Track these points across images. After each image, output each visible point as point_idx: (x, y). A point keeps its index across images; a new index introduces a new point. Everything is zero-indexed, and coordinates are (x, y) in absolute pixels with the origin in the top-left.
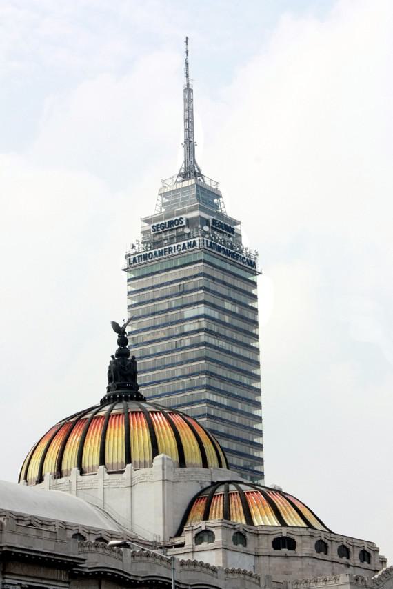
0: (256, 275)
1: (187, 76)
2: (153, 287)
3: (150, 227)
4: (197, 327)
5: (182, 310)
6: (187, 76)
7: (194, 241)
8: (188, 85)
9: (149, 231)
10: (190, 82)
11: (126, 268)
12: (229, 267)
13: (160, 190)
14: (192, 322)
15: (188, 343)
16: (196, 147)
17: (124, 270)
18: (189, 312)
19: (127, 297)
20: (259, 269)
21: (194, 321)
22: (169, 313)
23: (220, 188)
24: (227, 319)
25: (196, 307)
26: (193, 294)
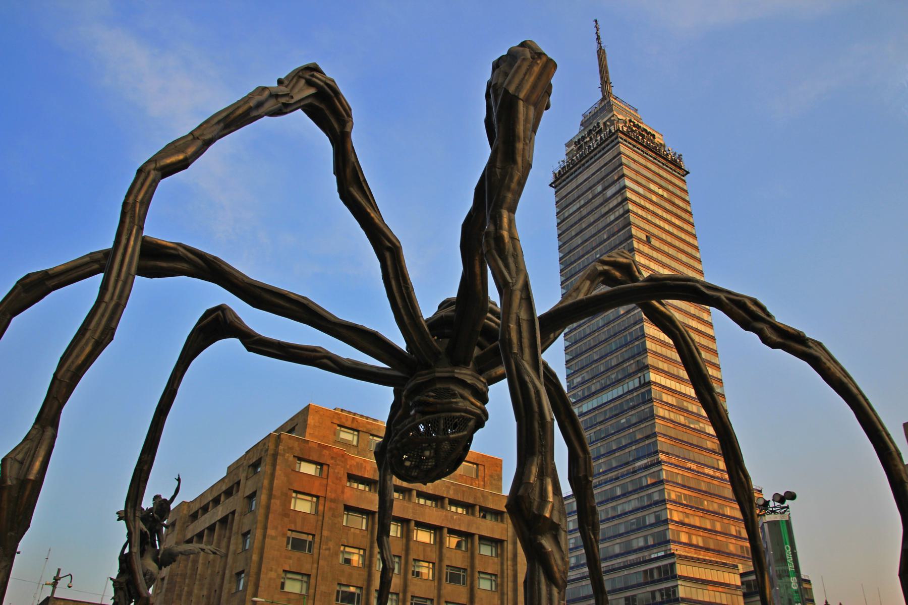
1: (599, 43)
2: (577, 187)
3: (573, 147)
4: (620, 199)
5: (604, 192)
6: (599, 43)
7: (610, 129)
9: (573, 149)
10: (602, 45)
11: (552, 181)
12: (653, 167)
13: (582, 121)
14: (615, 197)
17: (551, 185)
18: (609, 192)
19: (555, 206)
20: (685, 165)
21: (617, 196)
22: (593, 201)
24: (654, 198)
25: (618, 182)
26: (613, 173)
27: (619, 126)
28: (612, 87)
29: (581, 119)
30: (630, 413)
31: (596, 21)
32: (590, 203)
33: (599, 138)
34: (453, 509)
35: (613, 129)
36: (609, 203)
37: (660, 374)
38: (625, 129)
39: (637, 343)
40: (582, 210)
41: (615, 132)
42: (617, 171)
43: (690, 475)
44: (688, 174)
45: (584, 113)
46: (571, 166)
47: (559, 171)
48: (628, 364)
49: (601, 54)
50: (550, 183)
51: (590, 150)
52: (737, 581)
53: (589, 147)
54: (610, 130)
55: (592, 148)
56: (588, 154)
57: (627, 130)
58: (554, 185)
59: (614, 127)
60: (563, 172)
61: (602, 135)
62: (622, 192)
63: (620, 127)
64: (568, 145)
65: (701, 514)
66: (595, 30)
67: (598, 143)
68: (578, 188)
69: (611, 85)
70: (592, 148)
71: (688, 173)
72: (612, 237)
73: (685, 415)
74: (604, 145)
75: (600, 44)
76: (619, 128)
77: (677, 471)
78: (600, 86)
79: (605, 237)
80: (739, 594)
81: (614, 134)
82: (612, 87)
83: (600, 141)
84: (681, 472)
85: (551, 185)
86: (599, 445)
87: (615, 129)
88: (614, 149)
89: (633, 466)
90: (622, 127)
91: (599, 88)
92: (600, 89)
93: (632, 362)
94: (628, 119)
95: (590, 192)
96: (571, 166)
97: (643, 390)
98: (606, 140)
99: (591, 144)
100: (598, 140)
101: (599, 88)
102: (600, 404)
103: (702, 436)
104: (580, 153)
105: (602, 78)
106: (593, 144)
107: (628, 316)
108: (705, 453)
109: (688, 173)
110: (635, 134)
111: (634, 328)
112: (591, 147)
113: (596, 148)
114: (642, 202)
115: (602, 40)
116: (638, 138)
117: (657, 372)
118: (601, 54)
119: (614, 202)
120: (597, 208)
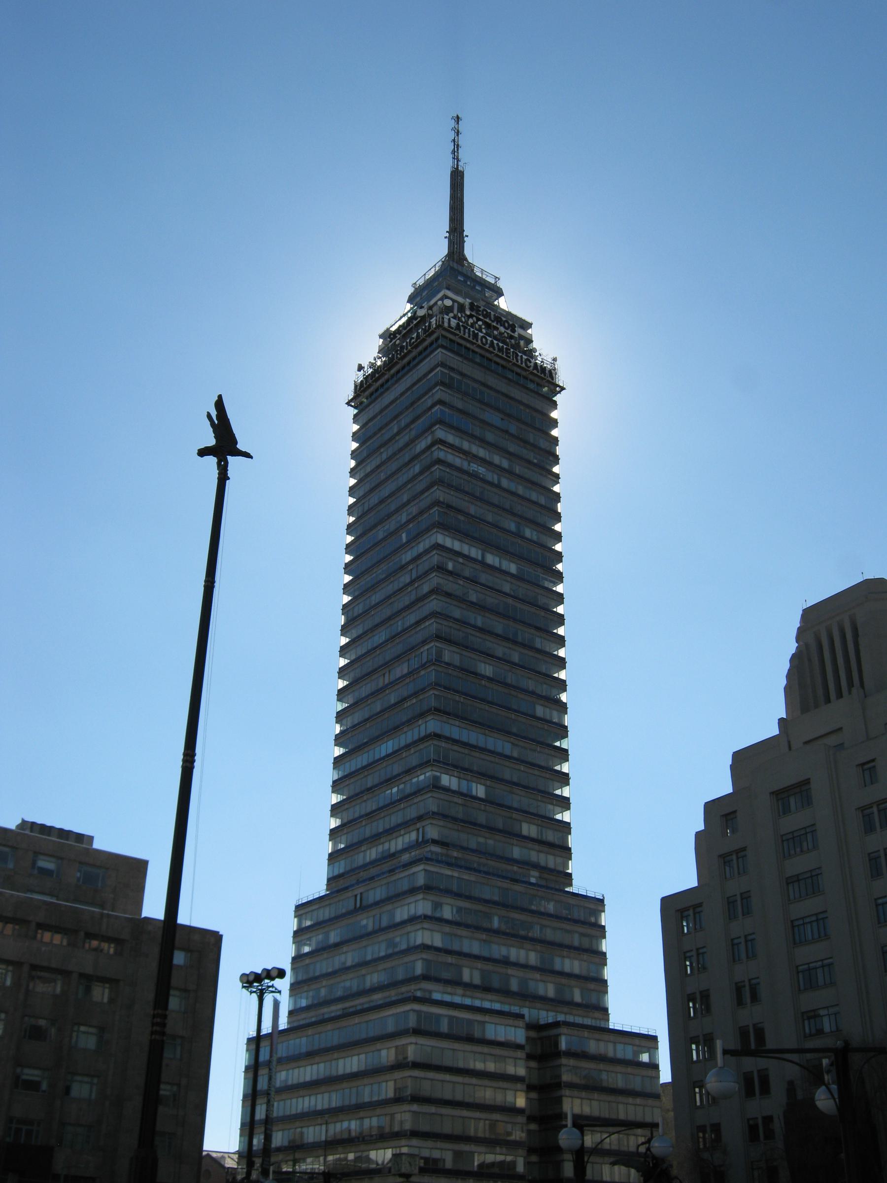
0: (559, 392)
1: (456, 159)
2: (381, 411)
4: (429, 440)
5: (412, 426)
6: (456, 159)
8: (458, 165)
10: (460, 163)
11: (351, 397)
15: (417, 469)
16: (466, 239)
17: (348, 404)
20: (562, 378)
22: (397, 438)
23: (500, 284)
24: (490, 437)
25: (430, 413)
27: (443, 318)
28: (467, 236)
29: (411, 290)
30: (404, 780)
31: (458, 119)
32: (394, 441)
33: (415, 335)
34: (47, 936)
35: (435, 322)
36: (416, 445)
37: (451, 721)
38: (454, 322)
39: (423, 673)
40: (382, 450)
41: (435, 329)
42: (431, 393)
43: (473, 878)
44: (564, 391)
45: (414, 282)
46: (377, 375)
47: (362, 381)
48: (409, 704)
49: (457, 179)
50: (347, 401)
51: (402, 354)
52: (518, 1035)
53: (402, 348)
54: (430, 323)
55: (405, 351)
56: (399, 359)
57: (458, 324)
58: (353, 404)
59: (436, 320)
60: (366, 384)
61: (420, 331)
62: (433, 430)
63: (446, 320)
64: (381, 336)
65: (484, 937)
66: (452, 135)
67: (413, 342)
68: (383, 414)
69: (465, 234)
70: (405, 351)
71: (563, 389)
72: (413, 501)
73: (488, 783)
74: (420, 348)
75: (458, 160)
76: (443, 322)
77: (449, 873)
78: (447, 235)
79: (405, 498)
80: (519, 1056)
81: (433, 332)
82: (467, 236)
83: (416, 341)
84: (456, 874)
85: (348, 404)
86: (364, 823)
87: (436, 324)
88: (432, 356)
89: (399, 859)
90: (449, 320)
91: (446, 237)
92: (447, 240)
93: (414, 701)
94: (468, 301)
95: (395, 422)
96: (377, 375)
97: (421, 746)
98: (424, 340)
99: (405, 344)
100: (413, 338)
101: (446, 237)
102: (371, 760)
103: (514, 816)
104: (390, 356)
105: (452, 220)
106: (407, 343)
107: (418, 629)
108: (515, 842)
109: (563, 389)
110: (472, 329)
111: (422, 650)
112: (404, 348)
113: (409, 352)
114: (466, 445)
115: (462, 154)
116: (475, 336)
117: (445, 719)
118: (457, 179)
119: (422, 445)
120: (401, 450)
